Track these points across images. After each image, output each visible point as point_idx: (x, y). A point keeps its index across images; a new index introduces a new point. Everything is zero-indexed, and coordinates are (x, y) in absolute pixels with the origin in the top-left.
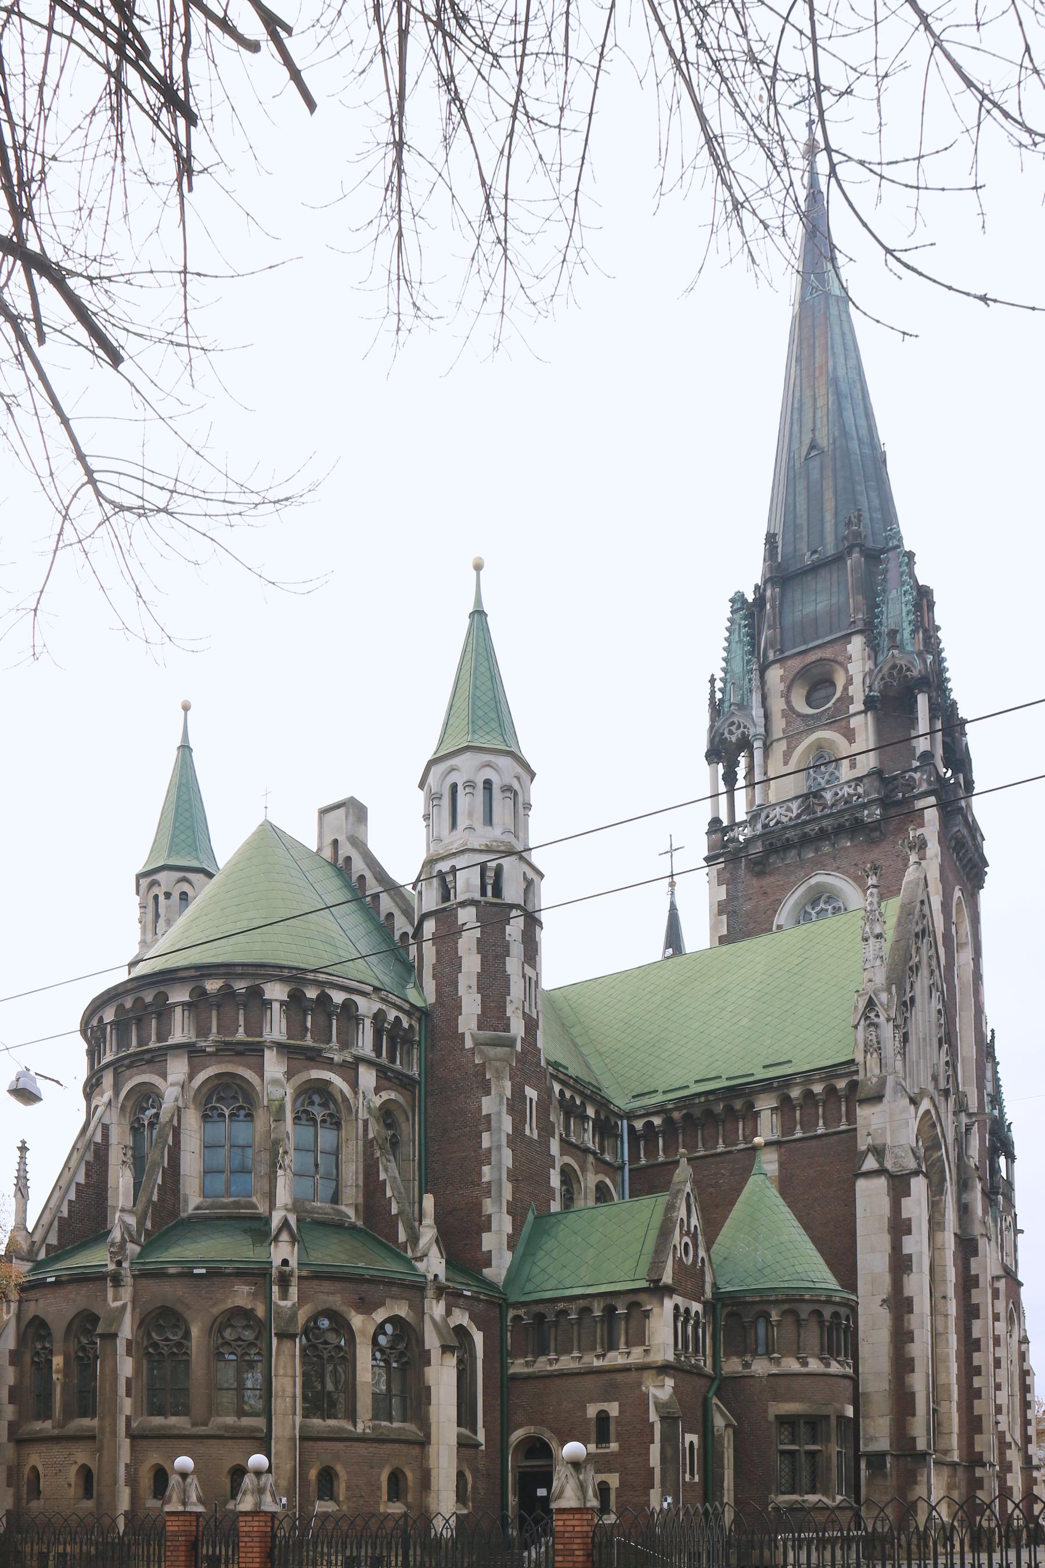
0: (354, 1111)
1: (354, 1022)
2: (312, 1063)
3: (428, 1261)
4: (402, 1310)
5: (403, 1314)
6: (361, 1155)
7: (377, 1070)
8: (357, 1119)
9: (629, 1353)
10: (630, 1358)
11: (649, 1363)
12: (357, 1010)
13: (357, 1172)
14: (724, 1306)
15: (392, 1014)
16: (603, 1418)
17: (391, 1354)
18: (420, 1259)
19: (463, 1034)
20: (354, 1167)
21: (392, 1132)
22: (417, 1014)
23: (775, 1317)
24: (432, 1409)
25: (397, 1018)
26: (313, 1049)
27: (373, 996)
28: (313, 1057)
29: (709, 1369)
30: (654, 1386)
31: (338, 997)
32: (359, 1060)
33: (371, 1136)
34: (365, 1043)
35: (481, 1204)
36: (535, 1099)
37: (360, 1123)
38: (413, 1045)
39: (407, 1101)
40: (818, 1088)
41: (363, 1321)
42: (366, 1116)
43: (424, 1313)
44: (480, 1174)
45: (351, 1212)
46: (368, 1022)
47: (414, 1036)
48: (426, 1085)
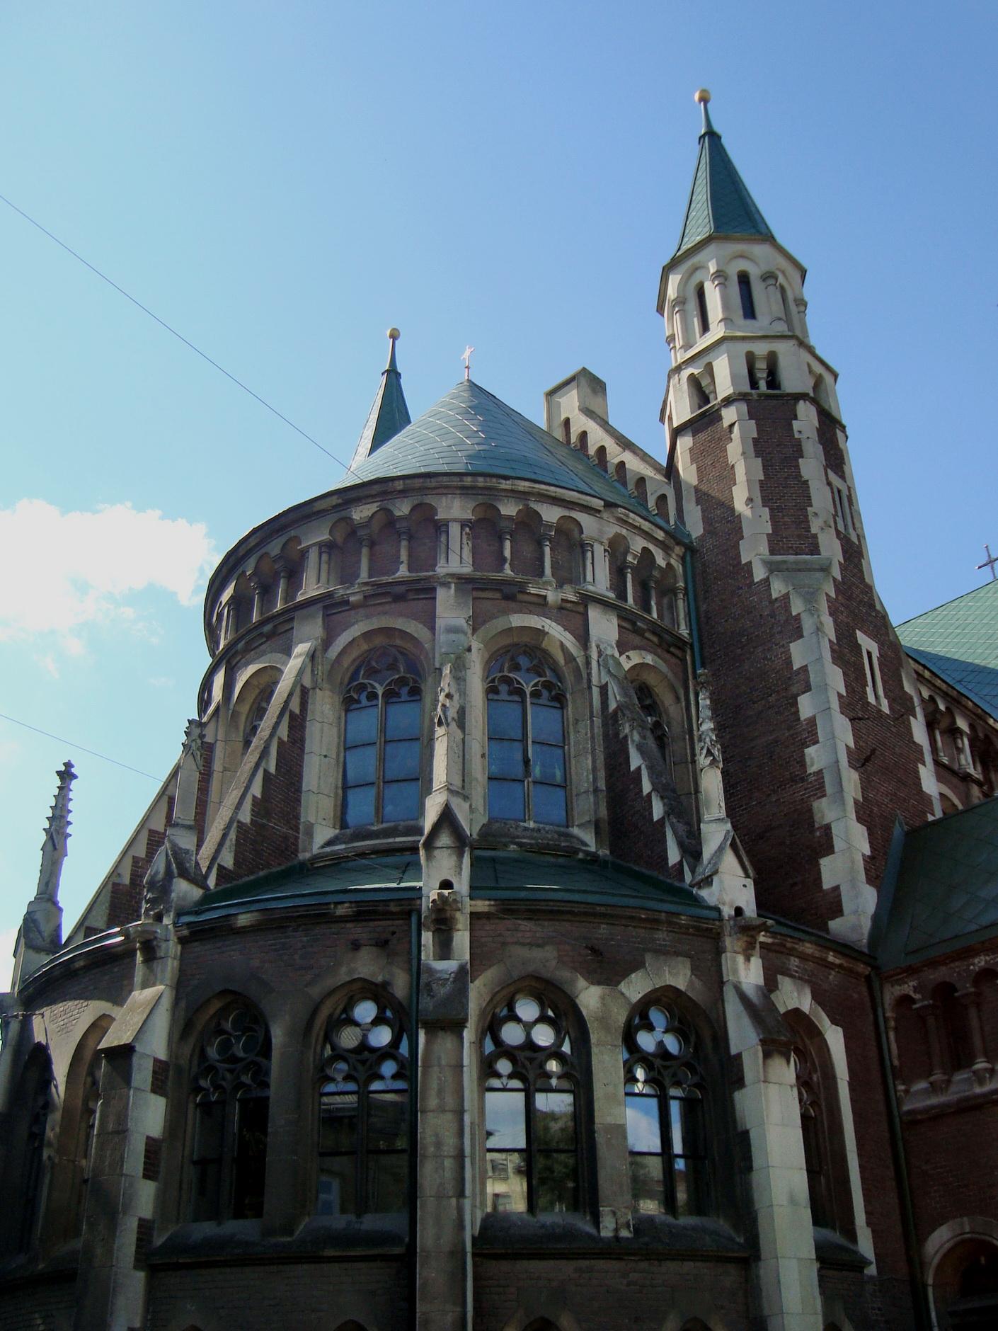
1: (579, 550)
2: (513, 605)
3: (721, 882)
4: (679, 976)
5: (682, 987)
6: (600, 740)
7: (619, 617)
8: (590, 688)
12: (581, 532)
13: (594, 770)
15: (638, 544)
17: (666, 1067)
18: (708, 881)
21: (654, 719)
22: (679, 550)
24: (756, 1177)
27: (605, 515)
28: (512, 595)
31: (551, 514)
32: (588, 599)
33: (613, 706)
34: (599, 578)
35: (810, 810)
36: (875, 654)
37: (596, 691)
38: (676, 595)
39: (675, 674)
41: (603, 998)
42: (605, 678)
43: (721, 983)
44: (802, 763)
45: (589, 838)
46: (599, 550)
47: (676, 582)
48: (701, 649)
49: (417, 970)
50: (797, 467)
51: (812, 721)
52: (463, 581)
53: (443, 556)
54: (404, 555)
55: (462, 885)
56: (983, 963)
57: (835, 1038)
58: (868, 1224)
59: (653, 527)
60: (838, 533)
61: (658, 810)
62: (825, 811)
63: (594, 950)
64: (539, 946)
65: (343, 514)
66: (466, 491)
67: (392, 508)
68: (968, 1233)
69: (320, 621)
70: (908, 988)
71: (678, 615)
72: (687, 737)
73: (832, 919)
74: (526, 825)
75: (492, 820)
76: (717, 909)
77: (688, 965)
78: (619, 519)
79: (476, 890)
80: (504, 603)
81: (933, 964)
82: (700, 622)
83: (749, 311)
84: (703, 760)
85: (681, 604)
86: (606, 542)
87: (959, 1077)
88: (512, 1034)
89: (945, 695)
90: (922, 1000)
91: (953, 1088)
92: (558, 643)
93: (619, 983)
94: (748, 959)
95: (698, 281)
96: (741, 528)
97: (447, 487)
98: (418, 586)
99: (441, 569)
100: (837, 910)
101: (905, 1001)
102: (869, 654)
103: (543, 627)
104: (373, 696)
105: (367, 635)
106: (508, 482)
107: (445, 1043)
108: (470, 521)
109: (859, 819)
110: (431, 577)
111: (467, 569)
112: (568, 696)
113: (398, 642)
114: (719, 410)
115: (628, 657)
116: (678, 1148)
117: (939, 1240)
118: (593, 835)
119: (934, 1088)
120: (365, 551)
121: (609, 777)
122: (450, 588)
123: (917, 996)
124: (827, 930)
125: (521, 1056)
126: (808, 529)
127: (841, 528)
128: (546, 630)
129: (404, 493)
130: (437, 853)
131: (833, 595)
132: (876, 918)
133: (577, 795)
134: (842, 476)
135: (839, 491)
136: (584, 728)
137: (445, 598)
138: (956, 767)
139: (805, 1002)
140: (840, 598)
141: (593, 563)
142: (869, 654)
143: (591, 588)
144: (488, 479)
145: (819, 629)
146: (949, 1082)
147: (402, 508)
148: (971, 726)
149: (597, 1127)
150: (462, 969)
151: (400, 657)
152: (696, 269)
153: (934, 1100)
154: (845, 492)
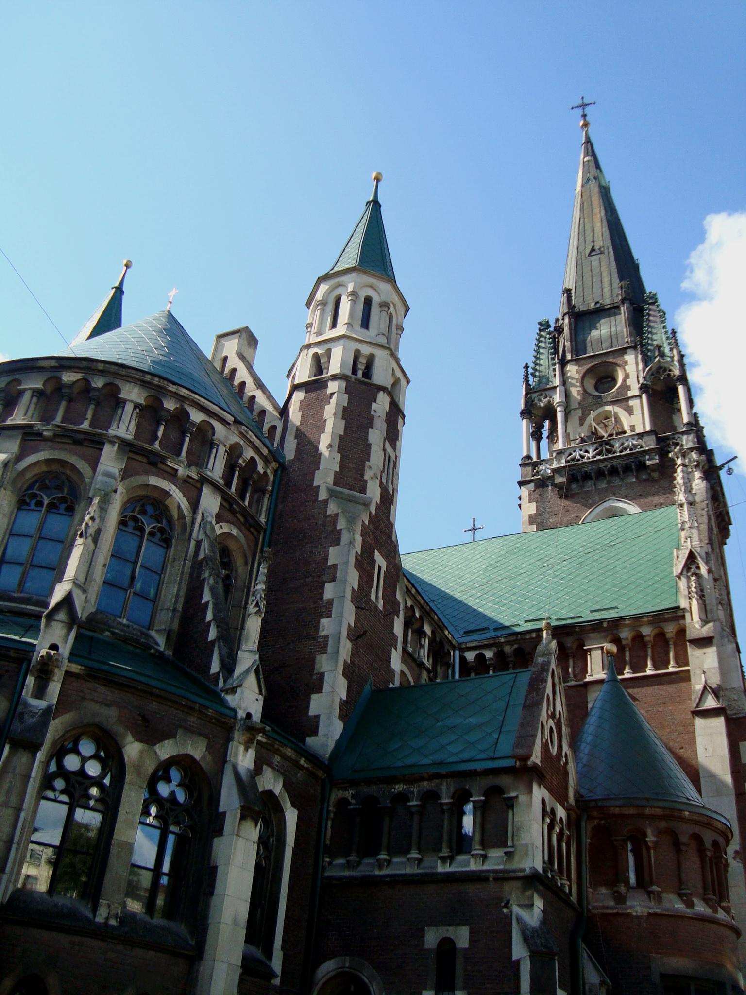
0: (188, 529)
2: (154, 469)
3: (242, 693)
4: (197, 750)
6: (186, 577)
7: (222, 498)
8: (189, 539)
9: (485, 857)
10: (487, 863)
11: (514, 871)
12: (214, 434)
13: (177, 596)
14: (590, 818)
15: (249, 453)
16: (447, 946)
17: (172, 810)
18: (233, 691)
19: (318, 487)
20: (176, 589)
21: (227, 572)
22: (274, 465)
23: (651, 838)
24: (214, 900)
25: (252, 458)
26: (155, 454)
27: (232, 428)
28: (155, 463)
29: (574, 898)
30: (519, 905)
31: (197, 417)
32: (205, 480)
33: (201, 556)
34: (216, 468)
35: (313, 662)
36: (384, 569)
37: (193, 544)
38: (264, 494)
40: (646, 631)
41: (141, 752)
42: (202, 536)
43: (225, 761)
46: (222, 449)
47: (267, 485)
48: (271, 534)
49: (16, 700)
50: (367, 433)
51: (330, 602)
52: (125, 446)
53: (116, 423)
54: (89, 415)
55: (65, 650)
56: (401, 789)
57: (291, 817)
58: (283, 948)
59: (262, 445)
60: (381, 483)
61: (212, 634)
62: (323, 663)
63: (144, 718)
64: (107, 705)
65: (57, 374)
66: (144, 384)
67: (90, 380)
68: (347, 968)
69: (18, 441)
70: (348, 794)
71: (261, 508)
72: (246, 590)
73: (310, 736)
74: (121, 620)
75: (98, 611)
76: (234, 711)
77: (205, 745)
78: (241, 433)
79: (74, 656)
80: (148, 466)
81: (369, 782)
82: (275, 516)
83: (365, 323)
84: (252, 609)
85: (266, 500)
86: (228, 446)
87: (367, 861)
88: (72, 762)
89: (421, 608)
90: (355, 804)
91: (361, 868)
92: (177, 504)
93: (155, 744)
94: (246, 749)
95: (338, 294)
96: (319, 462)
97: (132, 377)
98: (93, 438)
99: (112, 432)
100: (315, 732)
101: (342, 803)
102: (380, 568)
103: (170, 490)
104: (40, 504)
105: (48, 461)
106: (174, 386)
107: (23, 758)
108: (141, 405)
109: (344, 675)
110: (103, 434)
111: (129, 437)
112: (173, 541)
113: (68, 472)
114: (327, 381)
115: (221, 526)
116: (166, 868)
117: (328, 968)
118: (165, 639)
119: (349, 865)
120: (64, 404)
121: (186, 603)
122: (114, 446)
123: (353, 801)
124: (303, 741)
125: (73, 779)
126: (363, 475)
127: (384, 481)
128: (171, 493)
129: (102, 373)
130: (54, 624)
131: (367, 523)
132: (338, 743)
133: (161, 610)
134: (394, 448)
135: (389, 457)
136: (178, 565)
137: (109, 452)
138: (416, 656)
139: (278, 788)
140: (371, 526)
141: (215, 457)
142: (380, 568)
143: (209, 473)
144: (162, 381)
145: (351, 543)
146: (359, 863)
147: (98, 383)
148: (433, 632)
149: (114, 841)
150: (48, 710)
151: (66, 481)
152: (340, 285)
153: (346, 873)
154: (393, 458)
